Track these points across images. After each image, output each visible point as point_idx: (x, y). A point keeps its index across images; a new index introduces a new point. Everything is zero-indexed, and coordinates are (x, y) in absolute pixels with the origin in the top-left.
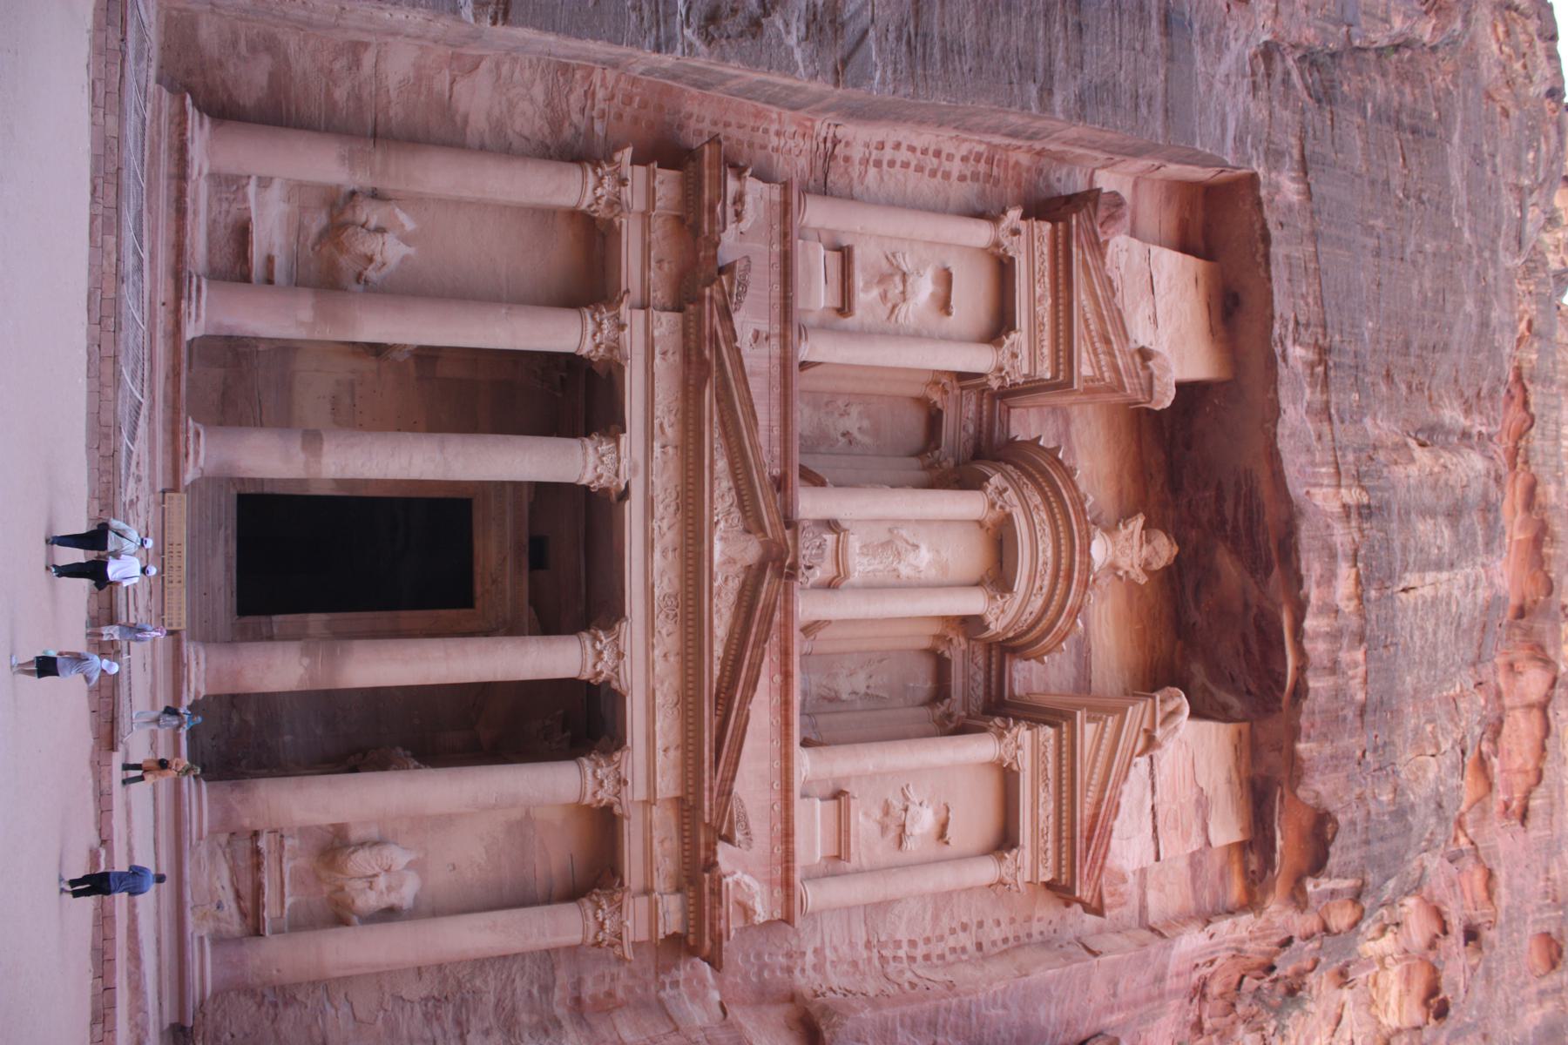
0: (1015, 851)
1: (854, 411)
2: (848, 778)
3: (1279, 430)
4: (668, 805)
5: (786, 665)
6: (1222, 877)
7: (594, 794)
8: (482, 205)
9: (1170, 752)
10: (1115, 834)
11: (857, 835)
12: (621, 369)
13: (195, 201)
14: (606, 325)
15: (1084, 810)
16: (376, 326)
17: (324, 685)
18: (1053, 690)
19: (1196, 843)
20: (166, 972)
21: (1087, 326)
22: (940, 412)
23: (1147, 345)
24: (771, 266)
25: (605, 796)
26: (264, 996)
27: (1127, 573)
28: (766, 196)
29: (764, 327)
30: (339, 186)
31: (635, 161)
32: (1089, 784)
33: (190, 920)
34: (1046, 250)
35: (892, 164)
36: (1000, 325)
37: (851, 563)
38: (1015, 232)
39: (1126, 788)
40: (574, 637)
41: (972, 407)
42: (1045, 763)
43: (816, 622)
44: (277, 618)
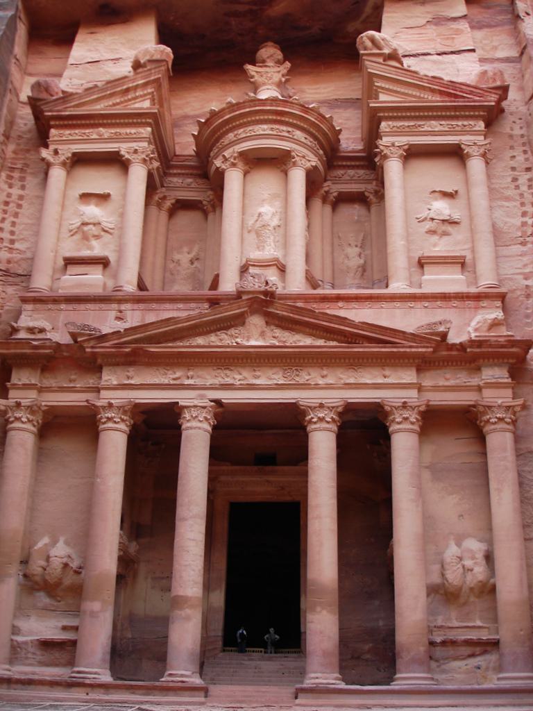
0: (462, 146)
1: (177, 257)
2: (409, 258)
4: (422, 375)
5: (332, 298)
6: (489, 8)
7: (412, 423)
8: (34, 494)
9: (401, 44)
10: (454, 80)
11: (449, 251)
12: (137, 405)
13: (26, 673)
14: (110, 416)
15: (435, 100)
16: (107, 561)
17: (334, 597)
18: (360, 124)
19: (464, 25)
20: (517, 701)
21: (118, 104)
22: (178, 201)
23: (131, 64)
24: (75, 310)
28: (29, 313)
29: (113, 314)
30: (20, 584)
32: (419, 97)
33: (485, 686)
34: (68, 132)
35: (12, 233)
36: (116, 161)
37: (268, 257)
38: (56, 152)
39: (422, 73)
40: (310, 435)
41: (175, 180)
42: (404, 127)
43: (306, 277)
44: (302, 630)
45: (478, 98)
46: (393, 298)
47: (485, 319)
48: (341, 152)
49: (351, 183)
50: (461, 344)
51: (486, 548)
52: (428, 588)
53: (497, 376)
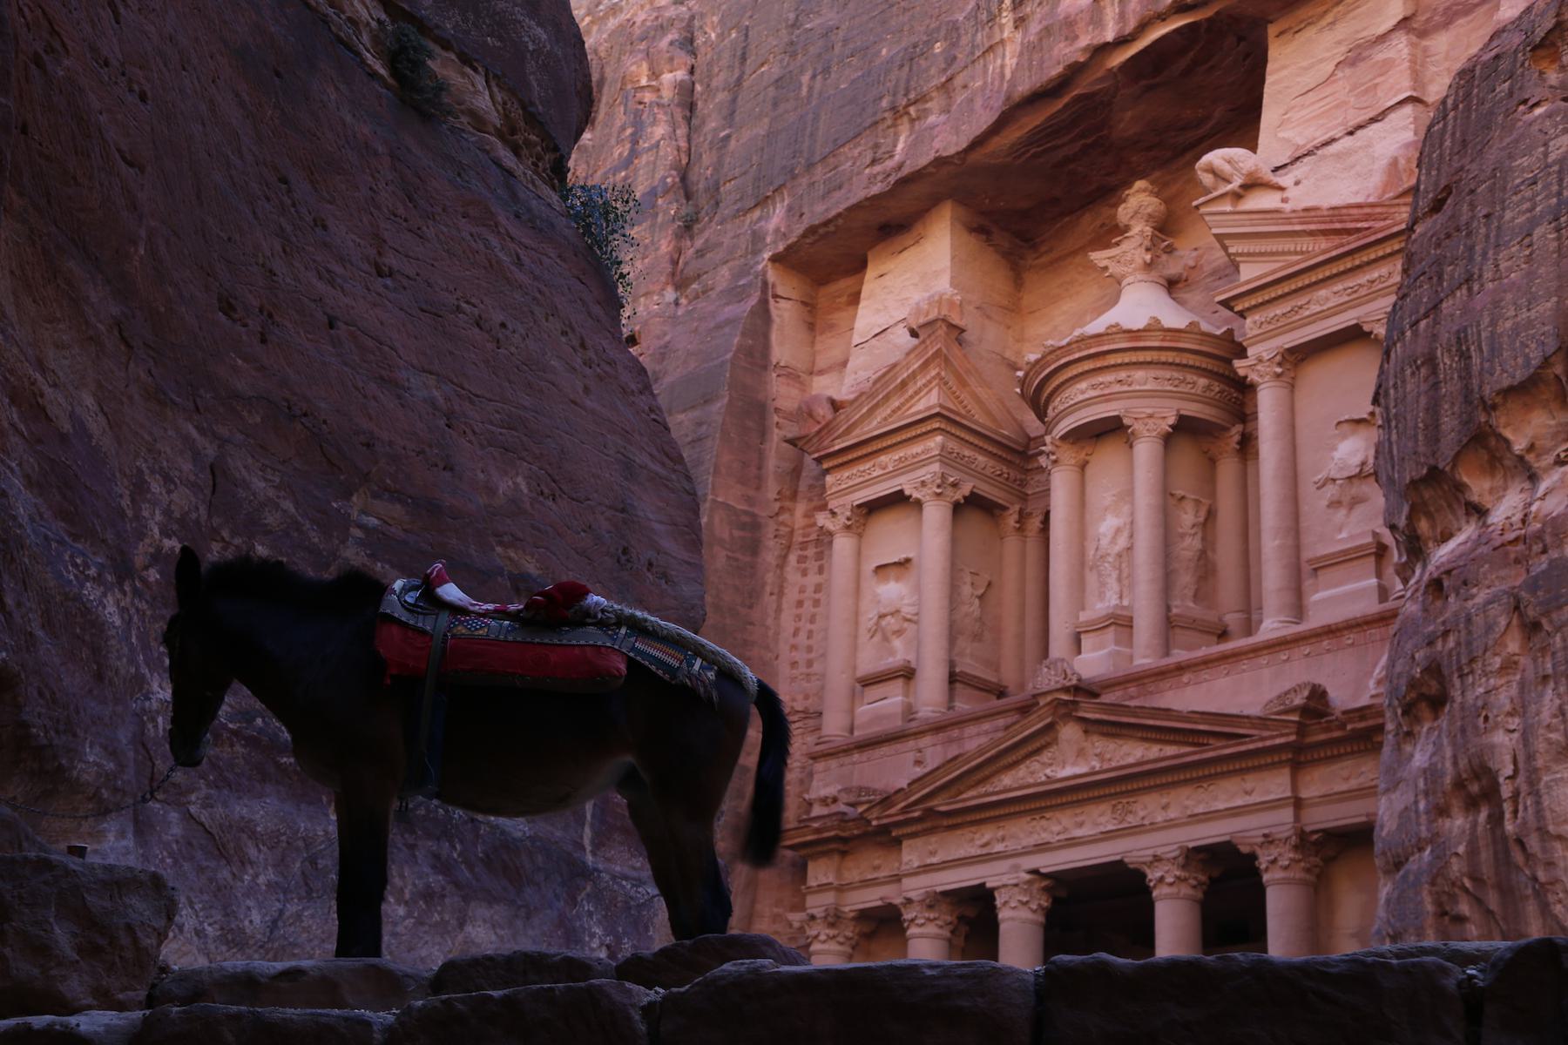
0: (1366, 328)
3: (952, 151)
4: (1308, 778)
7: (1286, 868)
10: (1337, 201)
12: (945, 894)
15: (1320, 248)
24: (869, 760)
25: (1287, 855)
27: (1148, 250)
29: (911, 756)
31: (803, 909)
38: (833, 514)
42: (1276, 318)
45: (1382, 224)
46: (1256, 650)
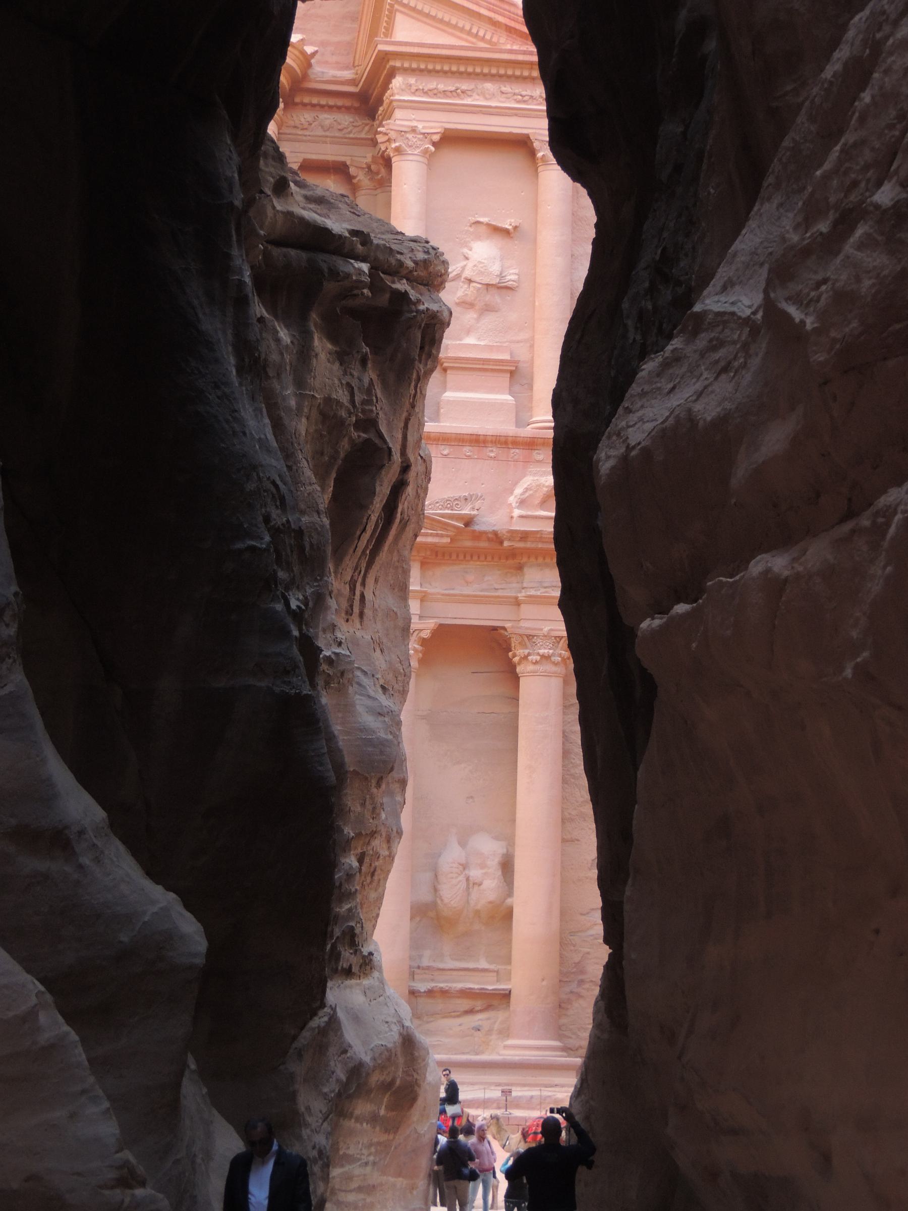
11: (490, 348)
20: (530, 1079)
26: (571, 992)
42: (435, 93)
47: (539, 485)
48: (310, 81)
49: (326, 142)
50: (495, 533)
51: (505, 851)
52: (411, 908)
53: (546, 585)
